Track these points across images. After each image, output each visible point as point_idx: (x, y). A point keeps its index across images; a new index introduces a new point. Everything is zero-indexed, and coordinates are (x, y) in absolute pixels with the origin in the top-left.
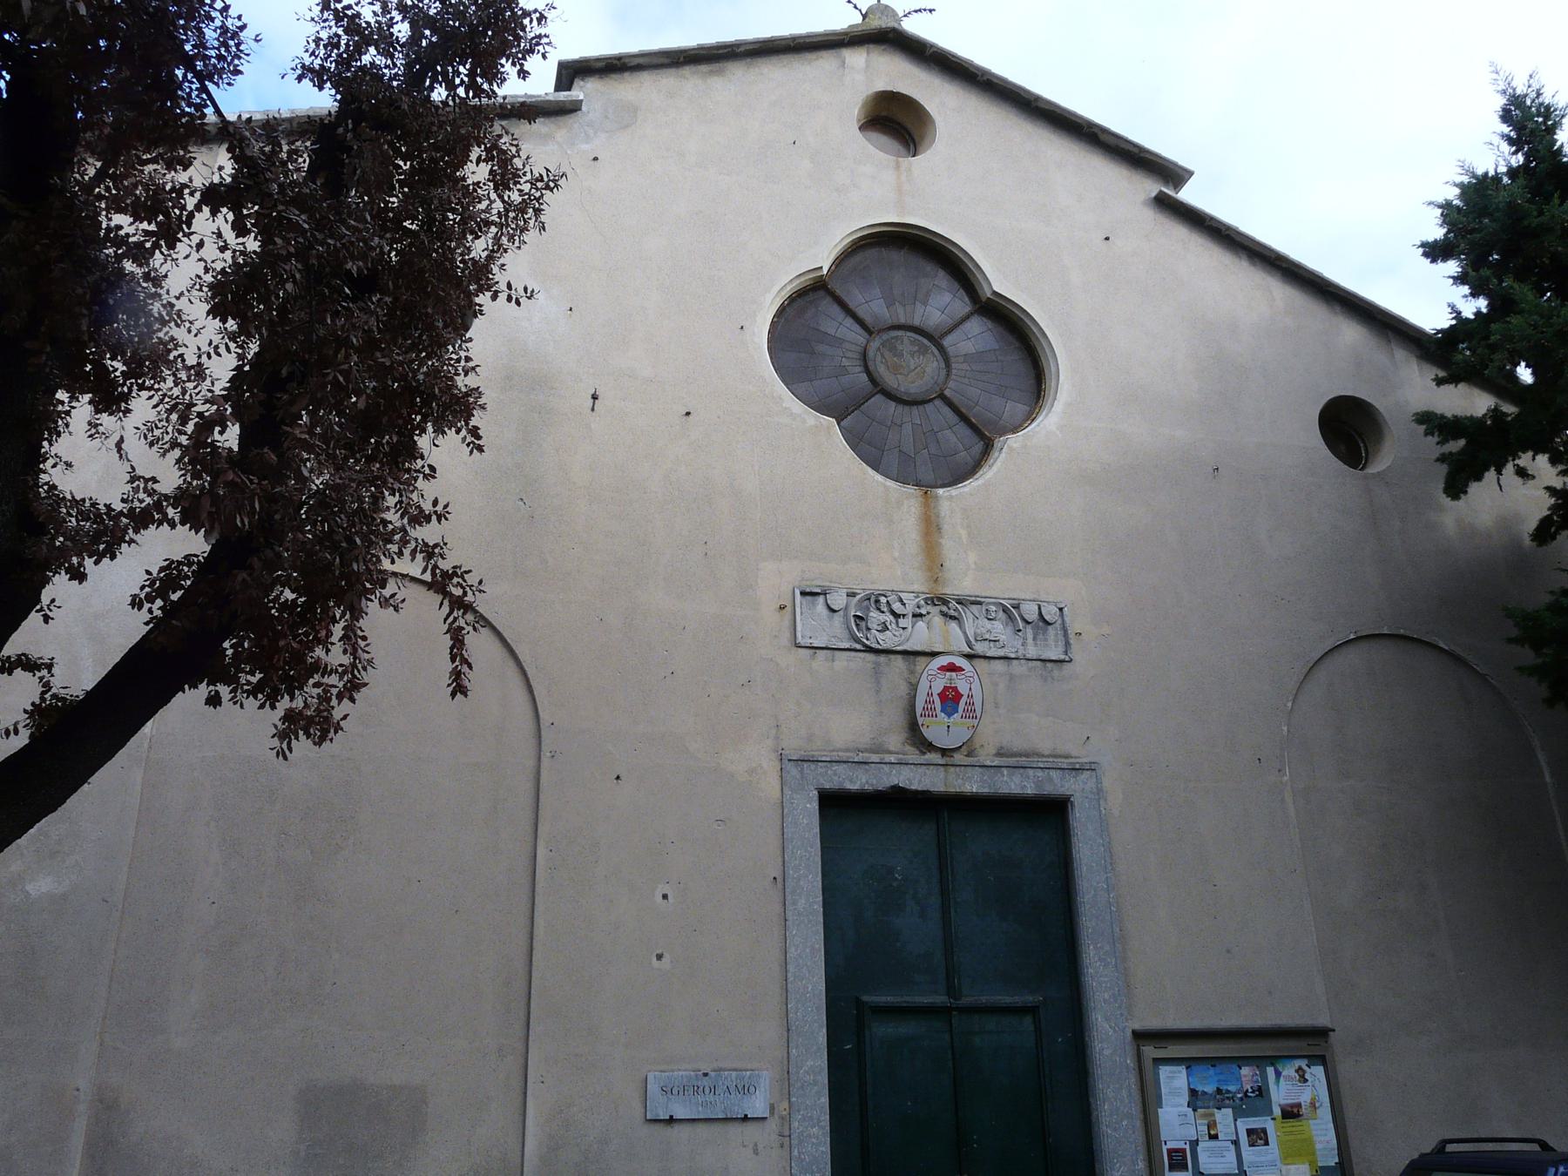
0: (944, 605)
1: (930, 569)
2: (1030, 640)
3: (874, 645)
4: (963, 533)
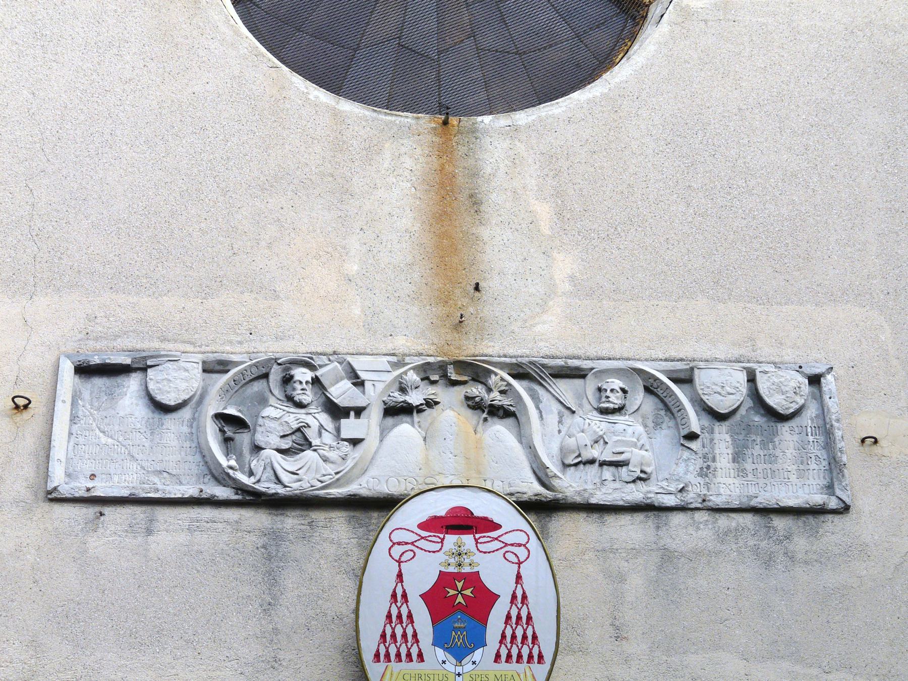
0: (481, 384)
1: (444, 298)
2: (724, 461)
3: (268, 487)
4: (544, 211)
